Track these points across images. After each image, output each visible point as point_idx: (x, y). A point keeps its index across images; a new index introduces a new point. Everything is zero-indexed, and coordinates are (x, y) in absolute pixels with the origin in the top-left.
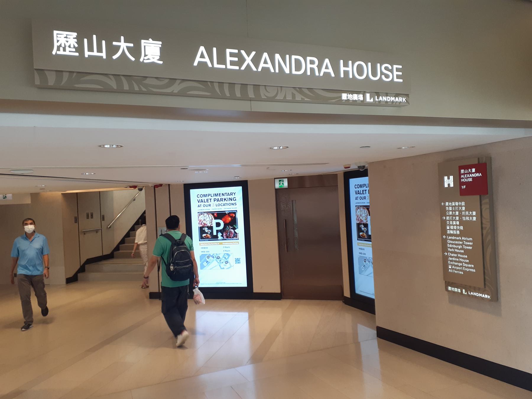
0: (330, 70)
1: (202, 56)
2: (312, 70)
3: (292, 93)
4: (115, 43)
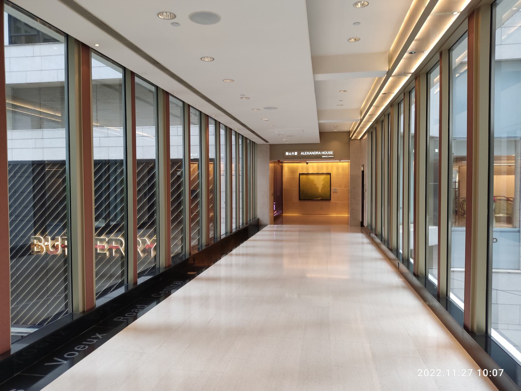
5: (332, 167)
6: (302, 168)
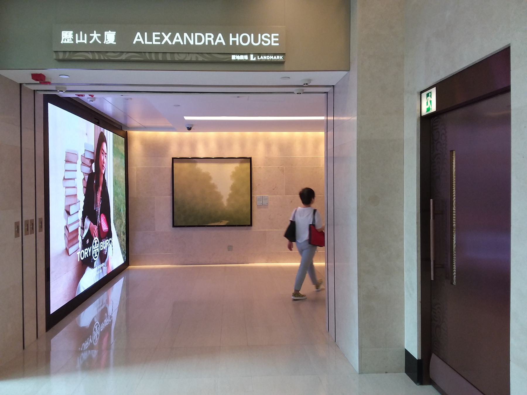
0: (222, 41)
1: (138, 38)
2: (209, 42)
3: (196, 57)
4: (91, 35)
5: (255, 142)
6: (181, 144)
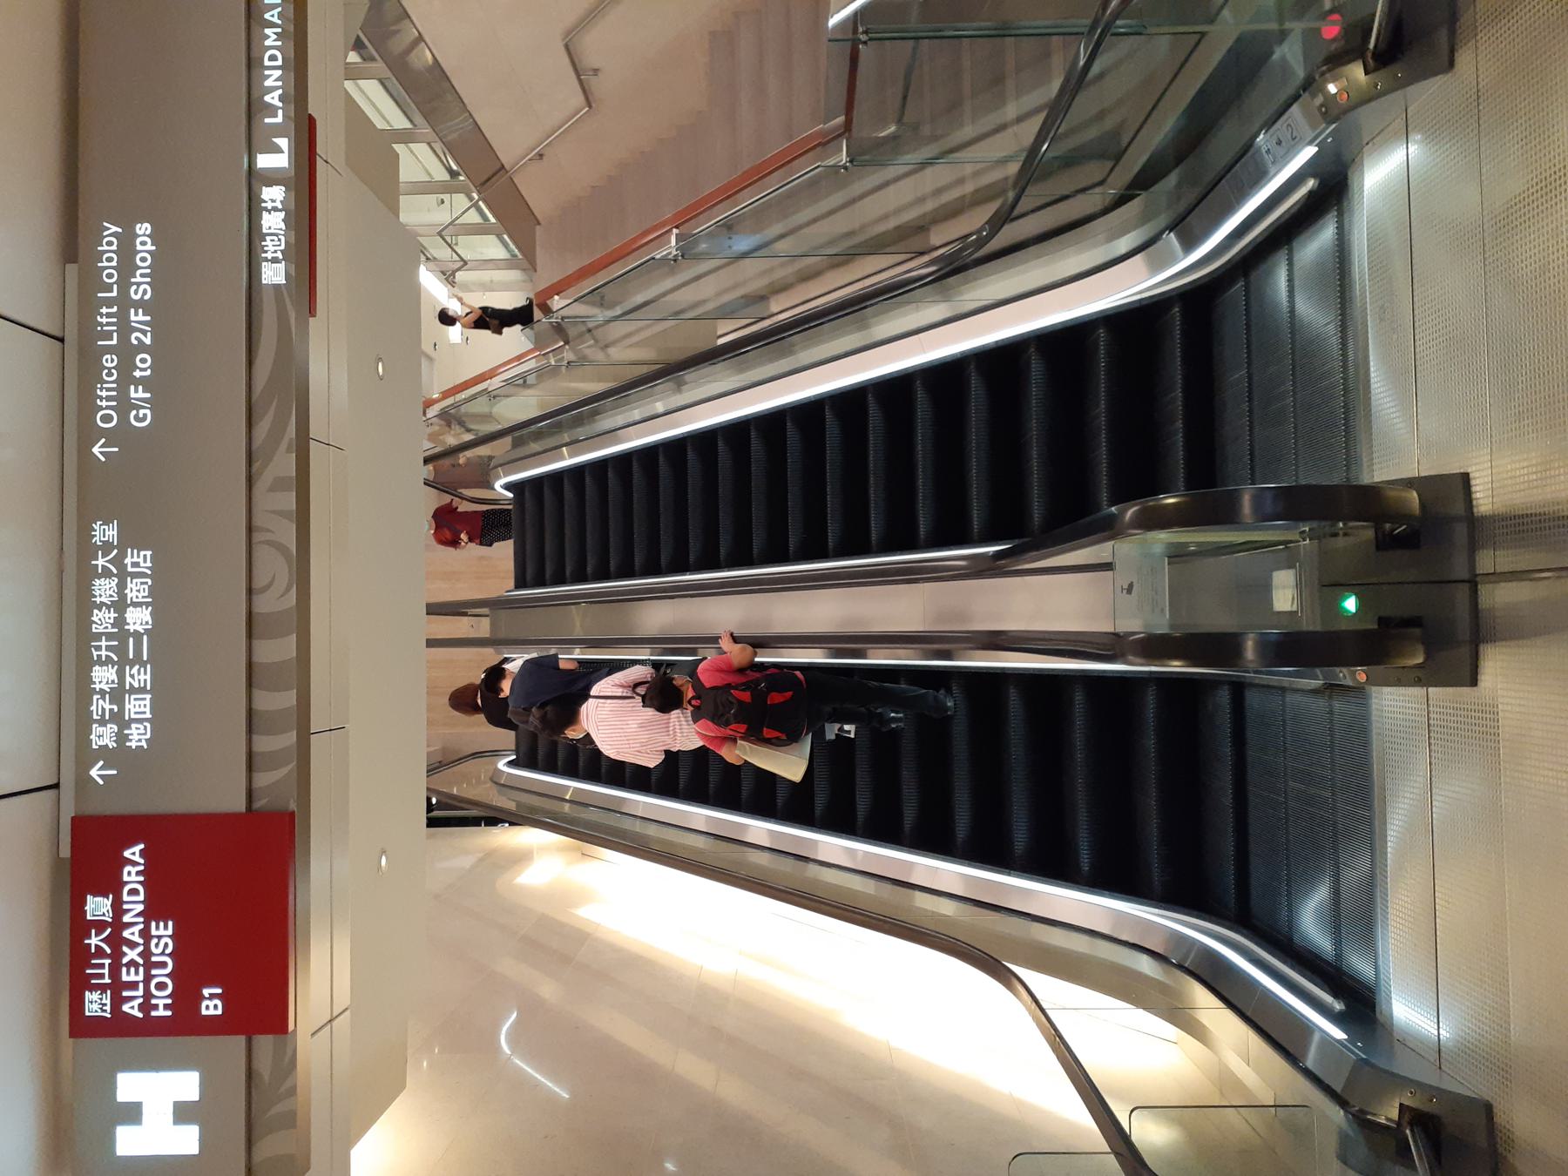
3: (271, 489)
